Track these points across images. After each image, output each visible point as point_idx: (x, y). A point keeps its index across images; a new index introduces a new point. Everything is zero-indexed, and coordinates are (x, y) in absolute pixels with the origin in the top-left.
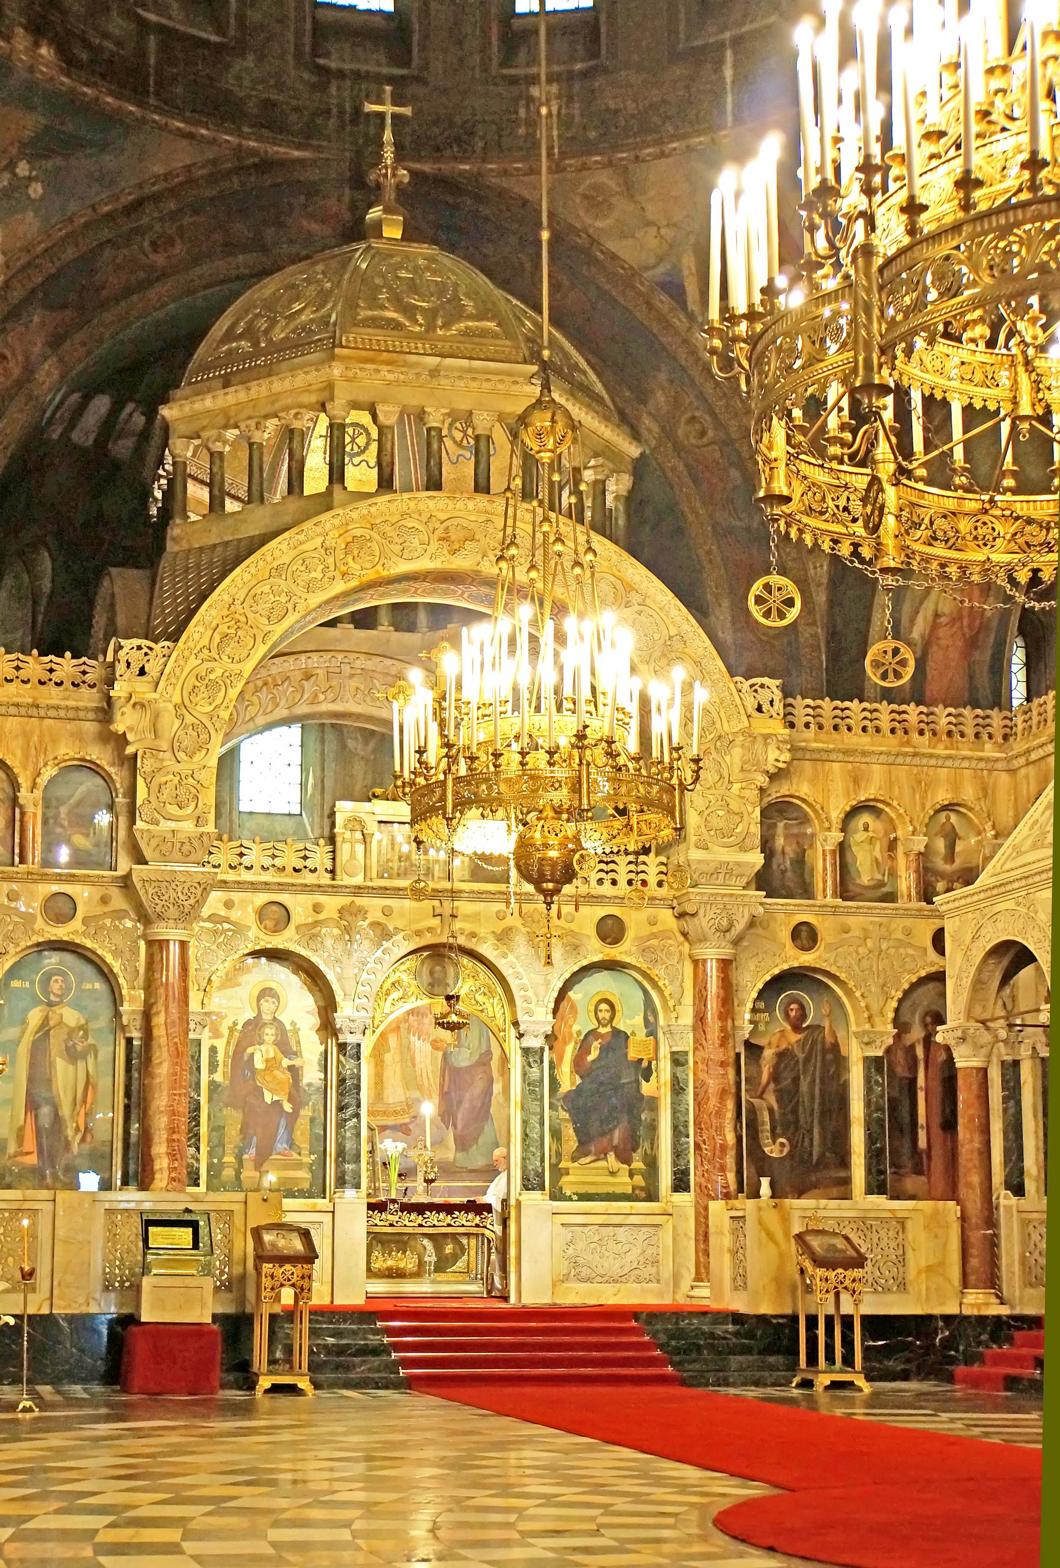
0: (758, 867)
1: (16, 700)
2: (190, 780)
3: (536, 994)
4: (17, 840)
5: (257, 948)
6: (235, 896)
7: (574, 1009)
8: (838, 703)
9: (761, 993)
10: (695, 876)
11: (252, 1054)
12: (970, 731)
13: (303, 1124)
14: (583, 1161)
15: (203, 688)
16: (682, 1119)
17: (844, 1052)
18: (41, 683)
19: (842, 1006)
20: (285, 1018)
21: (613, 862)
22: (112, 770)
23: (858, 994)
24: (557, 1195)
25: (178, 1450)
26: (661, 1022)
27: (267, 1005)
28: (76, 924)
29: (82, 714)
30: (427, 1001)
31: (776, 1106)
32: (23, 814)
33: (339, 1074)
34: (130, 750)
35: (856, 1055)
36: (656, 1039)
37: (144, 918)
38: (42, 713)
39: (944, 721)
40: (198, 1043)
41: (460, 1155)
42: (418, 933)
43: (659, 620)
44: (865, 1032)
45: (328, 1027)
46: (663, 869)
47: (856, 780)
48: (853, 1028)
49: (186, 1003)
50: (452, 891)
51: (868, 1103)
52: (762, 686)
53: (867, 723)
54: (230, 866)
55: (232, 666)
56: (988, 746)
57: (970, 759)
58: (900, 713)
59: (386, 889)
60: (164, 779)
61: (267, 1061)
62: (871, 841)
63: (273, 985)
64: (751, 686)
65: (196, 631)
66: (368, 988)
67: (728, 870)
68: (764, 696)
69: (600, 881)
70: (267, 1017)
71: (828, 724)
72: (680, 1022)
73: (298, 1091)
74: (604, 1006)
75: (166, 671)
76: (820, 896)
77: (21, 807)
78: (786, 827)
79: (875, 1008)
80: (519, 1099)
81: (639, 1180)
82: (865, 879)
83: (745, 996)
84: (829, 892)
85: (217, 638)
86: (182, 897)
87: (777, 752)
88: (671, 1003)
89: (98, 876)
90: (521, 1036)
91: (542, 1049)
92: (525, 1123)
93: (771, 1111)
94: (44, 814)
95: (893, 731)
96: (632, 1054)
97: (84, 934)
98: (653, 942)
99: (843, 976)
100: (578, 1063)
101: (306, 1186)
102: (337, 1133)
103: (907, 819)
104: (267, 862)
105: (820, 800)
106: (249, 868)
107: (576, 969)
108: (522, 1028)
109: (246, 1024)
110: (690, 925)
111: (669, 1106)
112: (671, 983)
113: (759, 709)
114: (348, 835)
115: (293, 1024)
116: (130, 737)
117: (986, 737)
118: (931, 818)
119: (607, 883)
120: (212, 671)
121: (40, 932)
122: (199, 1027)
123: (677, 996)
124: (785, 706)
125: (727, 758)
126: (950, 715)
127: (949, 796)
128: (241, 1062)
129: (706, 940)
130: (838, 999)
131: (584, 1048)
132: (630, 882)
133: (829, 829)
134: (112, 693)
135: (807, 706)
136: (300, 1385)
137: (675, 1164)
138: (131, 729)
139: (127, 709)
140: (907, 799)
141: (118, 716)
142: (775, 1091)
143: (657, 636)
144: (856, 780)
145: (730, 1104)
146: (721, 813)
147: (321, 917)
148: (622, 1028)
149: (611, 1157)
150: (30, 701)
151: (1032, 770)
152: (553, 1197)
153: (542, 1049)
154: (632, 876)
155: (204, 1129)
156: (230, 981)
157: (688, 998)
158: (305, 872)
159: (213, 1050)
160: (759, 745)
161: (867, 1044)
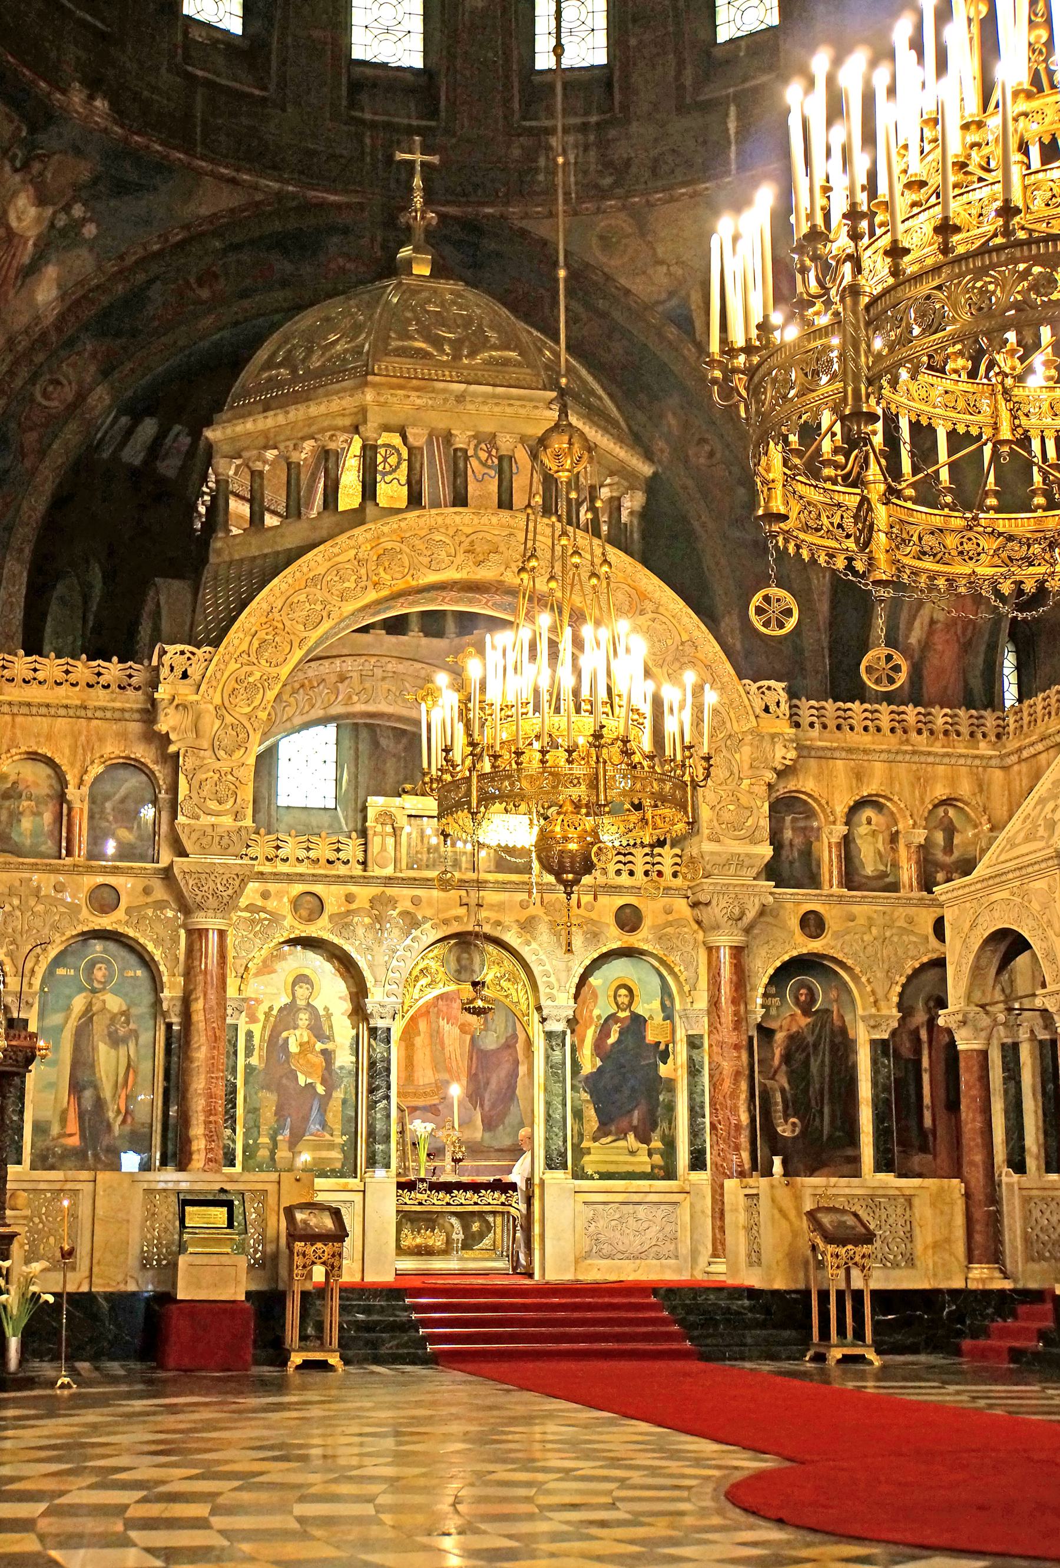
0: (767, 859)
1: (65, 702)
2: (229, 777)
3: (558, 980)
4: (64, 834)
5: (292, 936)
6: (272, 887)
7: (595, 995)
8: (840, 704)
9: (772, 978)
10: (708, 867)
11: (287, 1039)
12: (965, 730)
14: (604, 1140)
15: (242, 691)
16: (698, 1100)
17: (851, 1035)
18: (89, 686)
19: (849, 992)
20: (319, 1003)
21: (630, 854)
22: (155, 768)
23: (864, 979)
24: (579, 1174)
25: (211, 1426)
26: (678, 1006)
27: (301, 991)
28: (120, 914)
29: (127, 715)
30: (453, 987)
31: (786, 1086)
32: (70, 810)
33: (370, 1057)
34: (172, 749)
35: (863, 1038)
36: (673, 1022)
37: (186, 909)
38: (90, 714)
39: (940, 721)
40: (235, 1027)
41: (487, 1135)
42: (446, 922)
43: (671, 627)
44: (872, 1016)
45: (359, 1012)
46: (678, 860)
47: (859, 776)
48: (860, 1012)
49: (224, 989)
50: (478, 881)
51: (875, 1084)
52: (769, 688)
53: (868, 723)
54: (267, 859)
55: (270, 670)
56: (982, 744)
57: (966, 756)
58: (899, 714)
59: (415, 879)
60: (204, 776)
61: (301, 1045)
62: (874, 833)
63: (307, 972)
64: (759, 688)
65: (234, 635)
66: (397, 975)
67: (739, 862)
68: (771, 698)
69: (618, 872)
70: (301, 1003)
71: (832, 724)
72: (695, 1006)
73: (330, 1074)
74: (623, 992)
75: (208, 674)
76: (826, 886)
77: (69, 803)
78: (794, 820)
79: (880, 993)
80: (542, 1081)
81: (657, 1159)
82: (869, 870)
83: (758, 982)
84: (835, 882)
85: (256, 644)
86: (221, 888)
87: (784, 750)
88: (687, 988)
89: (141, 868)
90: (544, 1020)
91: (564, 1033)
92: (548, 1104)
93: (783, 1091)
94: (90, 810)
95: (893, 730)
96: (650, 1037)
97: (127, 923)
99: (849, 962)
100: (598, 1046)
101: (338, 1165)
102: (368, 1114)
103: (908, 813)
104: (302, 854)
105: (825, 795)
106: (286, 860)
107: (596, 955)
108: (545, 1013)
109: (281, 1010)
110: (705, 914)
111: (685, 1087)
112: (686, 969)
113: (767, 710)
114: (379, 828)
115: (326, 1009)
116: (172, 737)
117: (980, 736)
118: (930, 812)
119: (625, 875)
120: (251, 674)
121: (86, 921)
122: (236, 1013)
123: (692, 981)
124: (791, 707)
125: (737, 756)
126: (945, 715)
127: (947, 791)
128: (276, 1045)
130: (845, 984)
131: (604, 1031)
132: (646, 873)
133: (834, 823)
134: (156, 695)
135: (812, 707)
136: (331, 1361)
137: (691, 1143)
138: (174, 729)
139: (171, 710)
140: (907, 793)
141: (161, 717)
142: (787, 1073)
143: (670, 642)
144: (859, 776)
145: (744, 1086)
146: (731, 807)
147: (354, 906)
148: (640, 1011)
149: (631, 1137)
150: (78, 702)
151: (1024, 767)
152: (575, 1176)
153: (564, 1033)
154: (648, 867)
155: (240, 1111)
156: (267, 967)
157: (703, 983)
158: (338, 864)
159: (249, 1035)
160: (767, 745)
161: (873, 1027)
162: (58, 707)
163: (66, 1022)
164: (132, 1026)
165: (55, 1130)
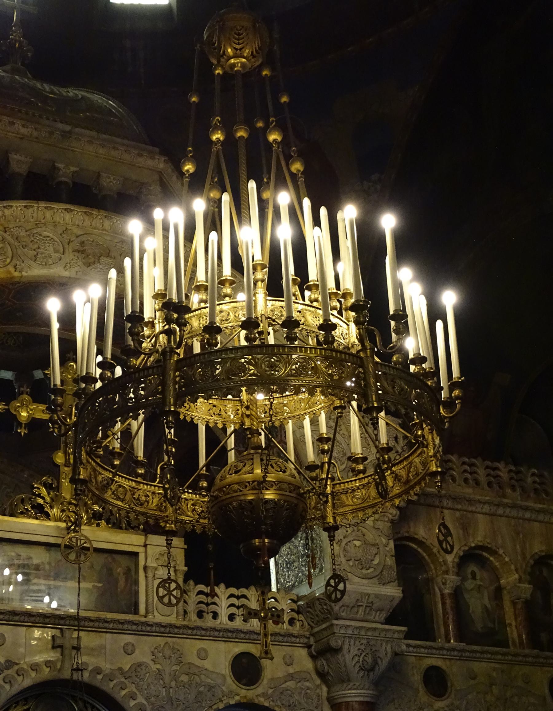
39: (530, 480)
98: (288, 684)
129: (349, 680)
133: (447, 572)
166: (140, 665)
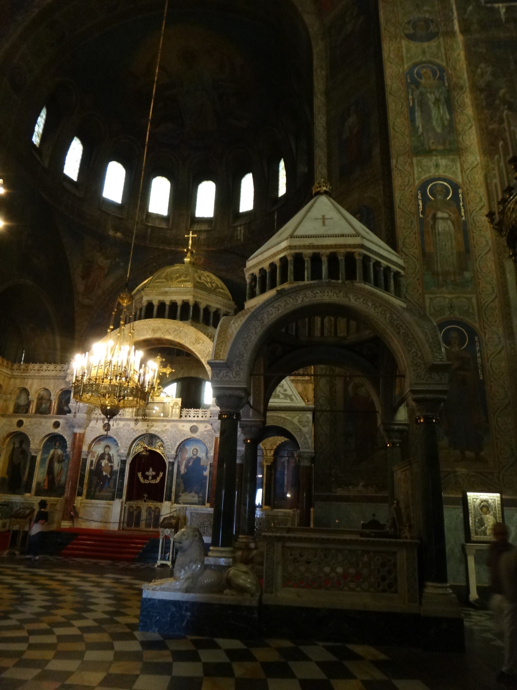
11: (101, 463)
13: (112, 482)
14: (186, 493)
18: (60, 371)
20: (111, 453)
24: (177, 502)
27: (107, 449)
38: (58, 378)
40: (86, 459)
61: (105, 464)
70: (106, 453)
74: (195, 450)
81: (200, 499)
100: (186, 467)
115: (113, 454)
128: (99, 464)
131: (188, 461)
141: (67, 378)
147: (119, 426)
148: (199, 456)
150: (55, 375)
155: (86, 481)
159: (92, 461)
162: (50, 376)
163: (48, 457)
164: (64, 458)
165: (42, 485)
166: (167, 429)
